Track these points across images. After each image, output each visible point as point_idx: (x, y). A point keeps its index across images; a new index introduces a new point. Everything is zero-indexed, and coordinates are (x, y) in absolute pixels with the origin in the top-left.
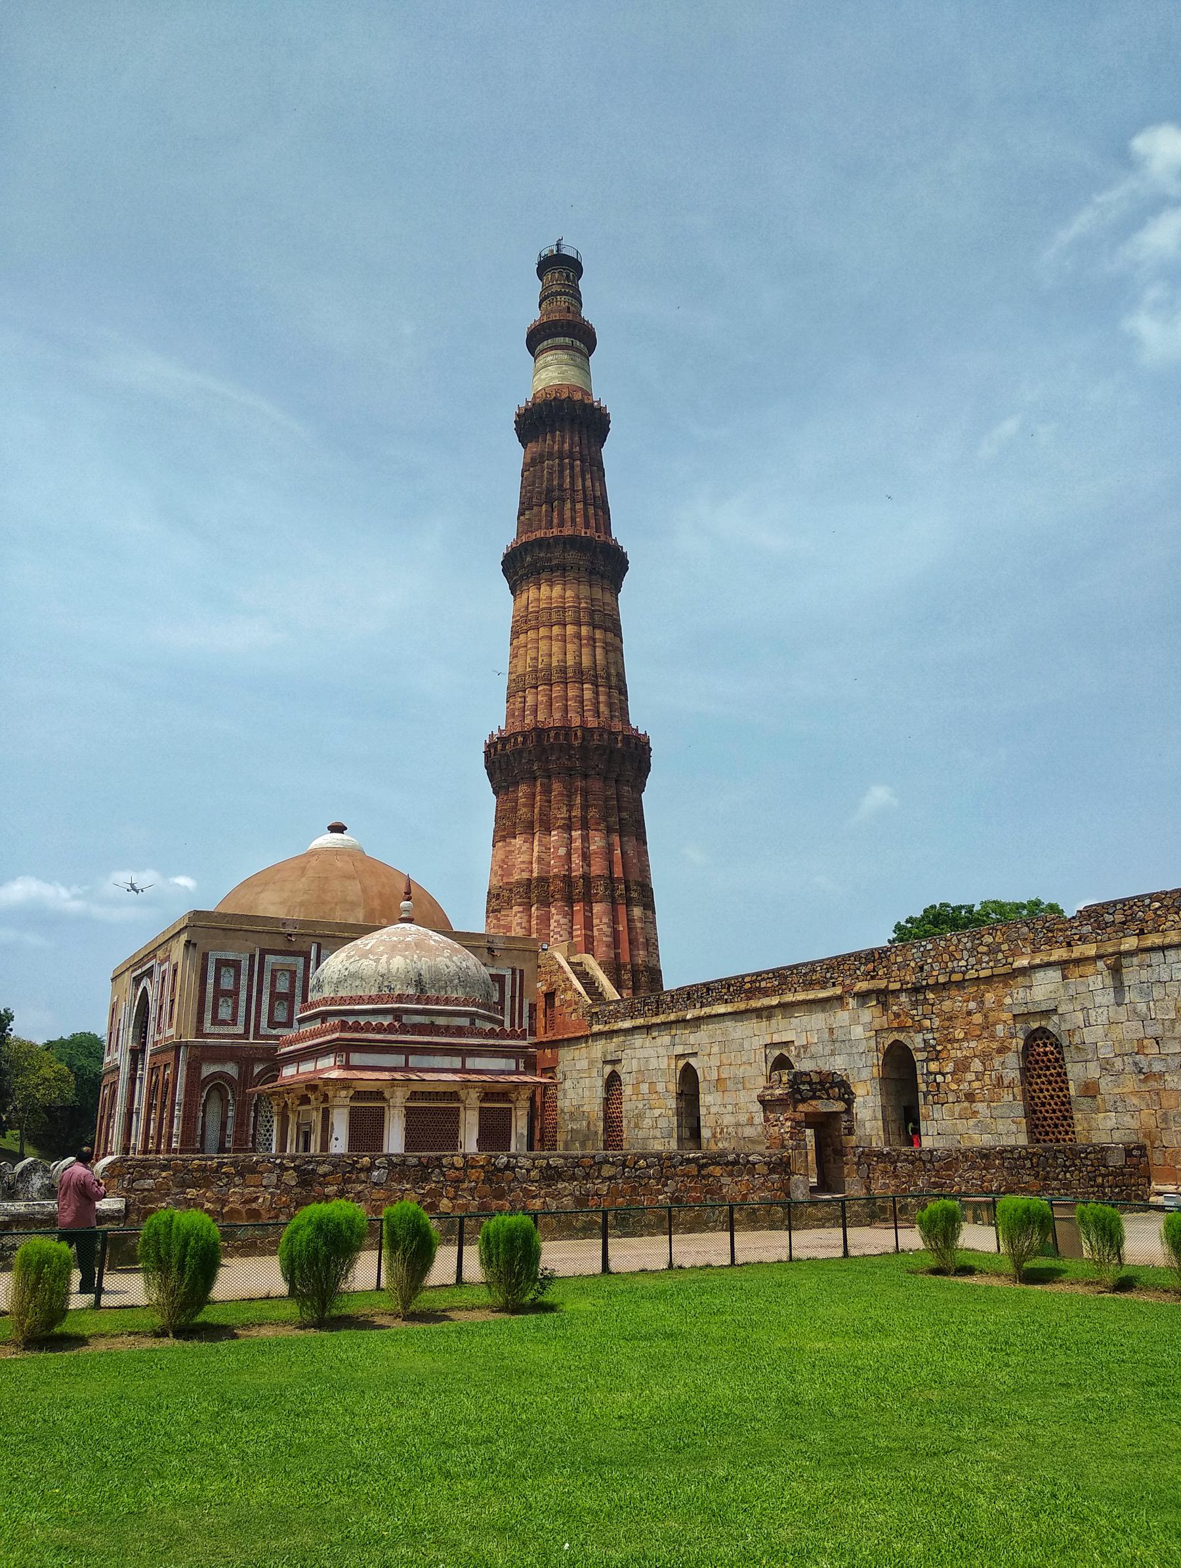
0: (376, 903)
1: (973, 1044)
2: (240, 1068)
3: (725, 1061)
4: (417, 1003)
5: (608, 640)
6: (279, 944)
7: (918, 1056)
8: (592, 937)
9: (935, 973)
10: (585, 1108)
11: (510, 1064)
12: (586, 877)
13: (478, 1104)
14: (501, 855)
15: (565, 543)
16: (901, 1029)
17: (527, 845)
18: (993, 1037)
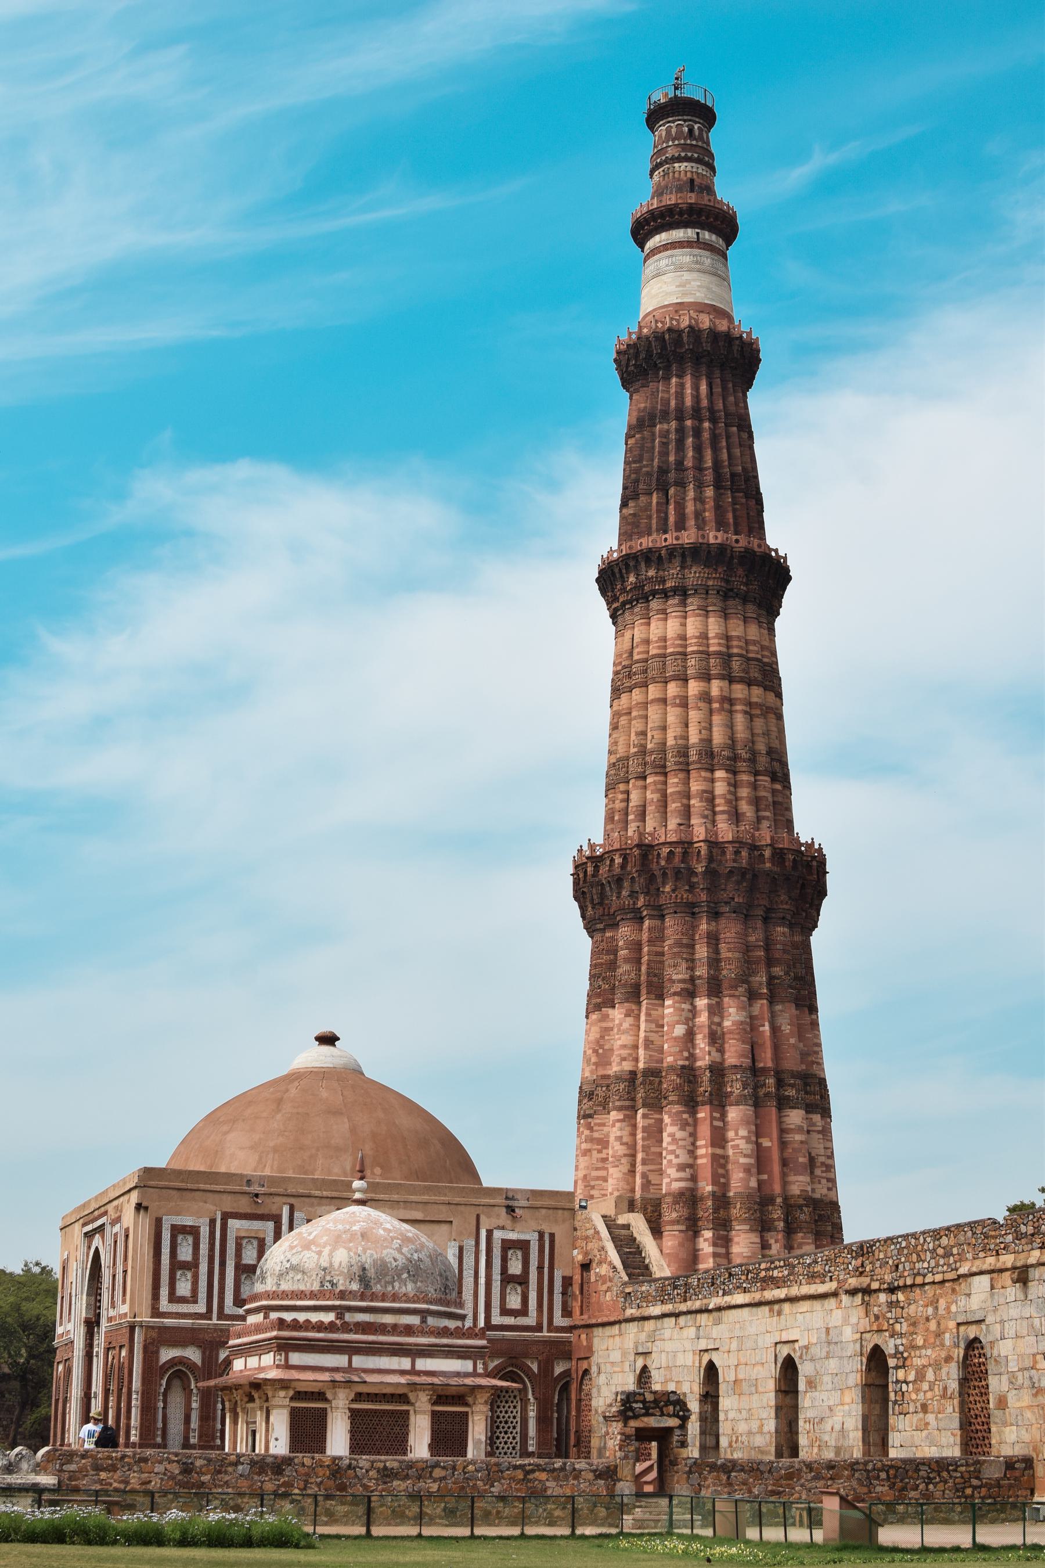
0: (368, 1148)
1: (929, 1352)
2: (204, 1353)
3: (743, 1360)
4: (362, 1300)
5: (755, 699)
6: (244, 1205)
7: (892, 1362)
8: (726, 1157)
9: (906, 1274)
11: (467, 1366)
12: (718, 1071)
13: (428, 1407)
14: (595, 1033)
15: (683, 556)
16: (879, 1331)
17: (630, 1020)
18: (942, 1345)
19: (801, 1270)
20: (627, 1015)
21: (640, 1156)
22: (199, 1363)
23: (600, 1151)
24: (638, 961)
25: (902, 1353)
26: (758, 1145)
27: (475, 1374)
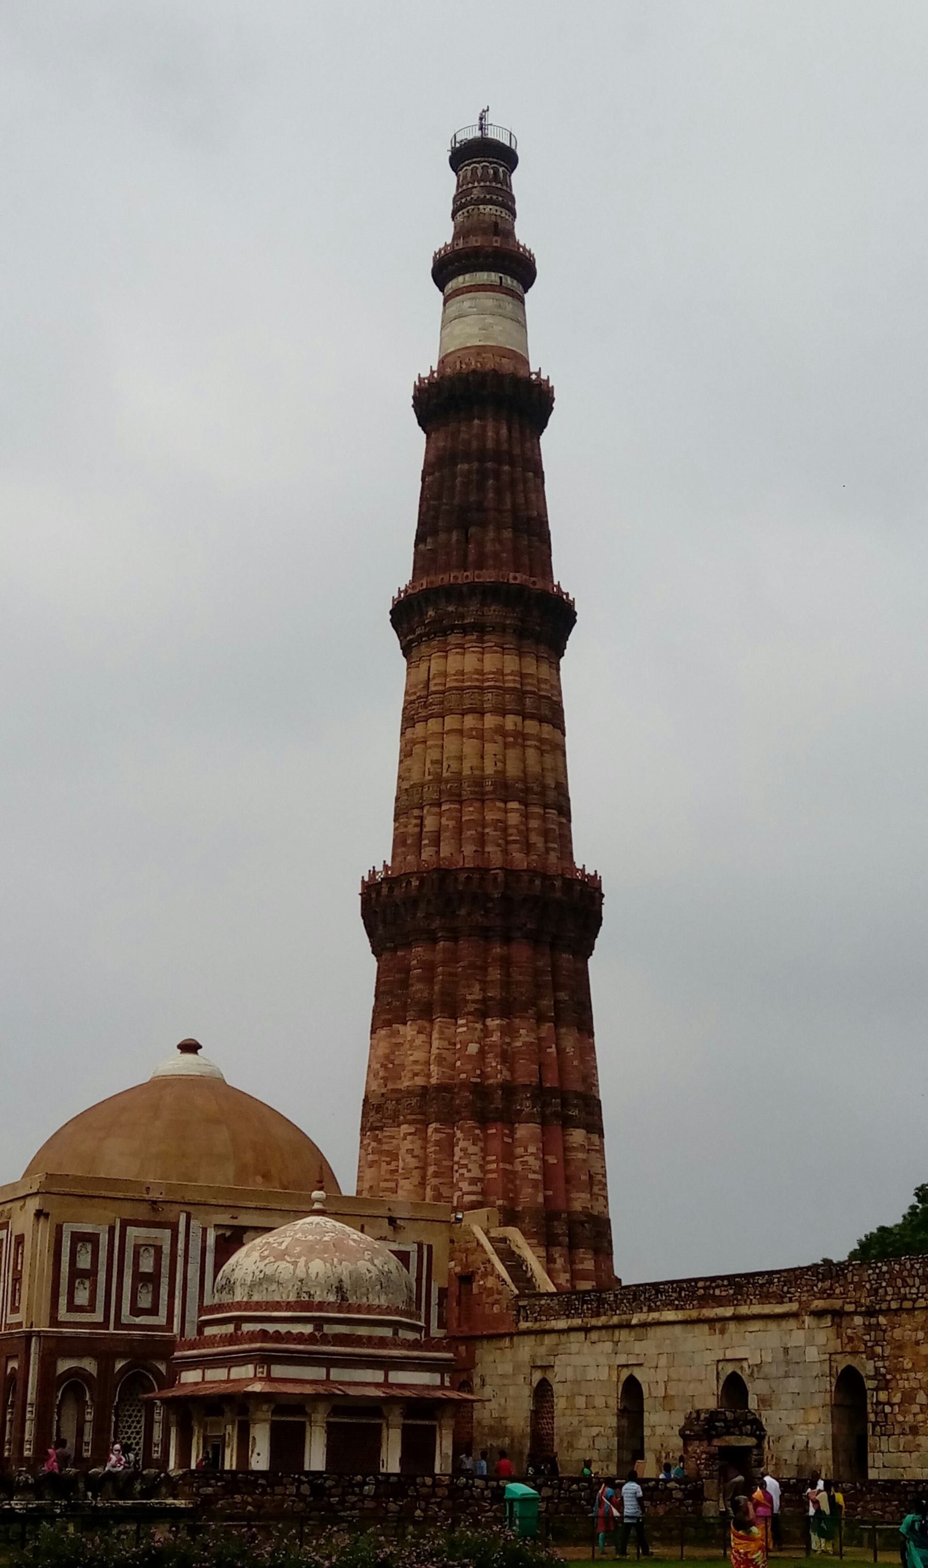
0: (249, 1157)
4: (339, 1312)
6: (143, 1212)
7: (870, 1384)
9: (888, 1298)
10: (509, 1422)
14: (382, 1050)
16: (854, 1353)
17: (422, 1037)
19: (751, 1290)
20: (418, 1033)
21: (431, 1169)
22: (95, 1375)
23: (388, 1163)
24: (429, 980)
25: (884, 1376)
26: (544, 1161)
27: (442, 1387)
